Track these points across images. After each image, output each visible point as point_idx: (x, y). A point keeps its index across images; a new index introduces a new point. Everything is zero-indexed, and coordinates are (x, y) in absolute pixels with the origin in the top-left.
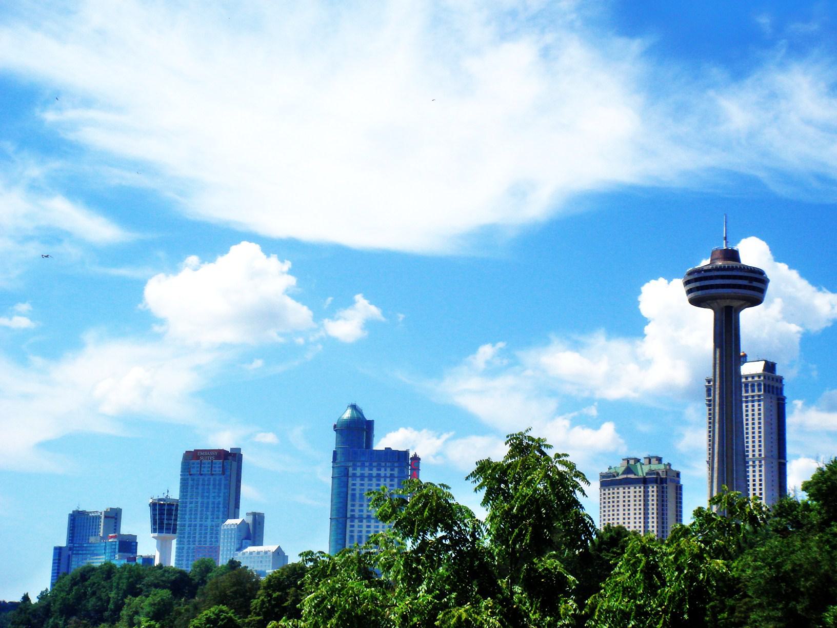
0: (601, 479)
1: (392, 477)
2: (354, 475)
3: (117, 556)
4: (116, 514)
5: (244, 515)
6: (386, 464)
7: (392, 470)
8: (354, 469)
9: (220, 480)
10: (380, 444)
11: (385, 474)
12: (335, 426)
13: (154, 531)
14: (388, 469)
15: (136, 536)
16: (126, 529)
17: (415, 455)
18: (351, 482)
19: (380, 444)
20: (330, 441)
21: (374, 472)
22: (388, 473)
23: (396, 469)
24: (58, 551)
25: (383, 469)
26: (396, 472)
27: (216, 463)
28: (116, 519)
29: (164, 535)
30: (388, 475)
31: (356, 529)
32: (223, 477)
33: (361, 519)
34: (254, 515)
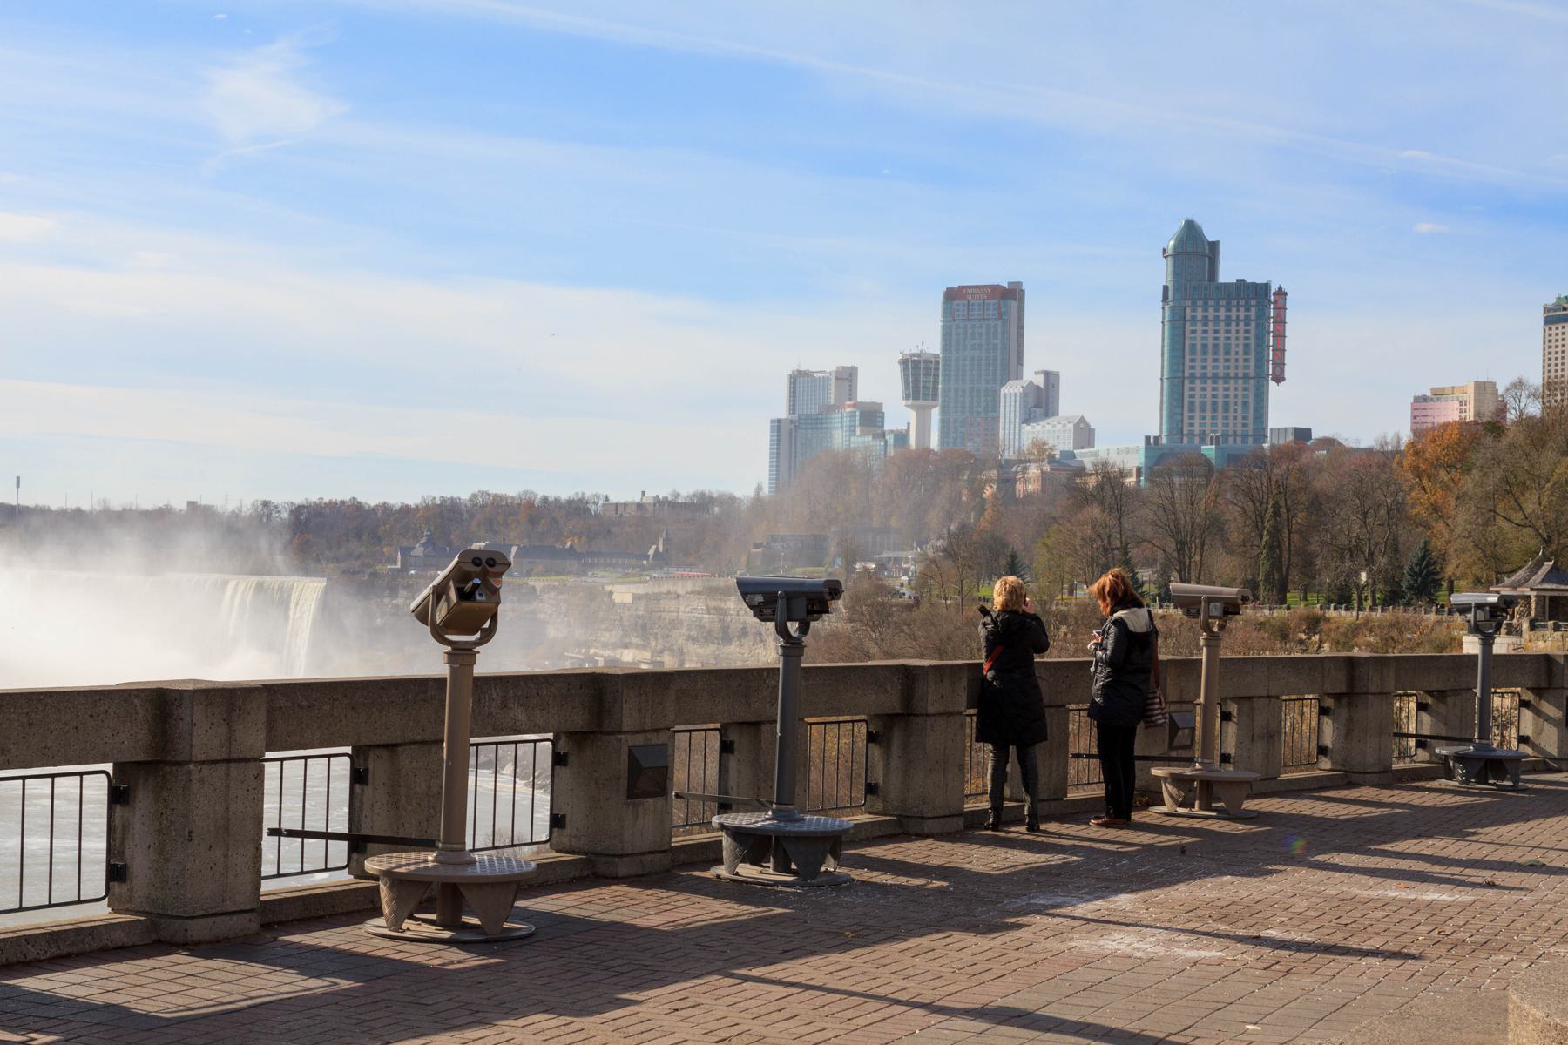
0: (1545, 313)
1: (1247, 320)
2: (1194, 319)
3: (858, 429)
4: (851, 375)
5: (1031, 372)
6: (1238, 303)
7: (1248, 310)
8: (1194, 311)
9: (996, 326)
10: (1228, 273)
11: (1238, 316)
12: (1164, 251)
13: (907, 397)
14: (1242, 309)
15: (881, 405)
16: (865, 394)
17: (1280, 289)
18: (1189, 327)
19: (1228, 273)
20: (1160, 273)
21: (1222, 313)
22: (1242, 314)
23: (1253, 309)
24: (777, 425)
25: (1234, 309)
26: (1253, 313)
27: (989, 304)
28: (851, 381)
29: (920, 402)
30: (1242, 317)
31: (1198, 392)
32: (999, 323)
33: (1204, 378)
34: (1047, 374)
